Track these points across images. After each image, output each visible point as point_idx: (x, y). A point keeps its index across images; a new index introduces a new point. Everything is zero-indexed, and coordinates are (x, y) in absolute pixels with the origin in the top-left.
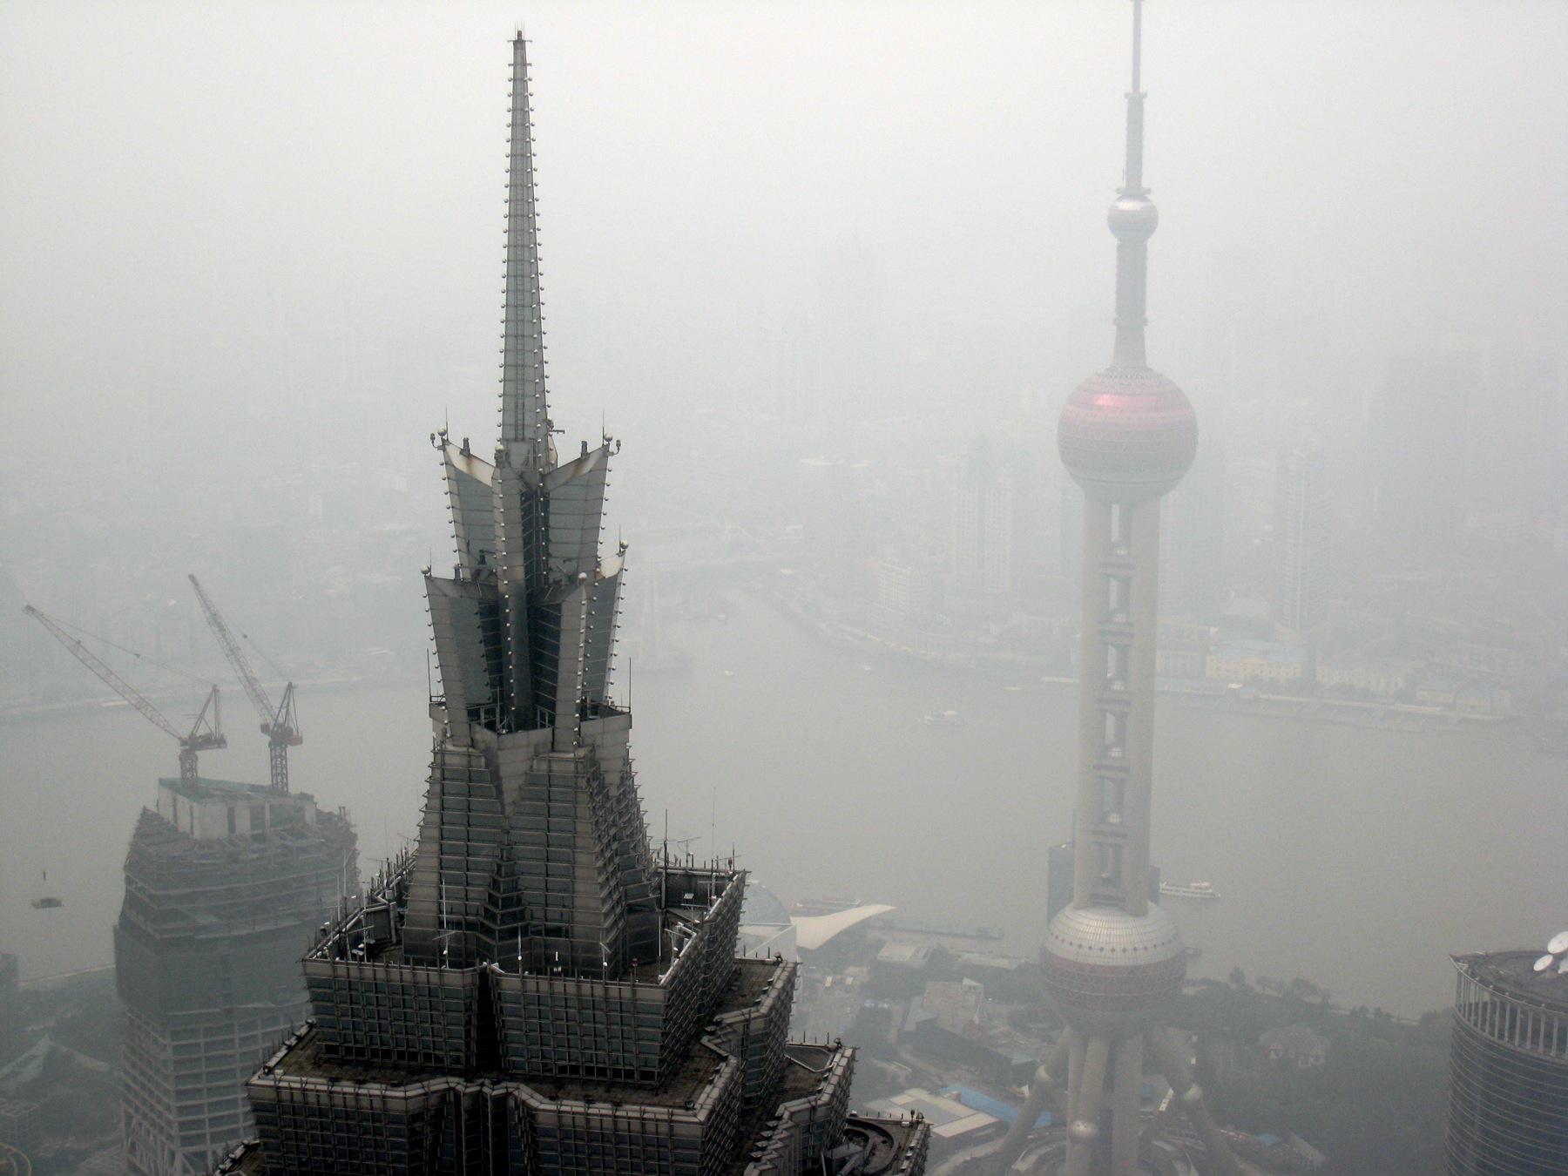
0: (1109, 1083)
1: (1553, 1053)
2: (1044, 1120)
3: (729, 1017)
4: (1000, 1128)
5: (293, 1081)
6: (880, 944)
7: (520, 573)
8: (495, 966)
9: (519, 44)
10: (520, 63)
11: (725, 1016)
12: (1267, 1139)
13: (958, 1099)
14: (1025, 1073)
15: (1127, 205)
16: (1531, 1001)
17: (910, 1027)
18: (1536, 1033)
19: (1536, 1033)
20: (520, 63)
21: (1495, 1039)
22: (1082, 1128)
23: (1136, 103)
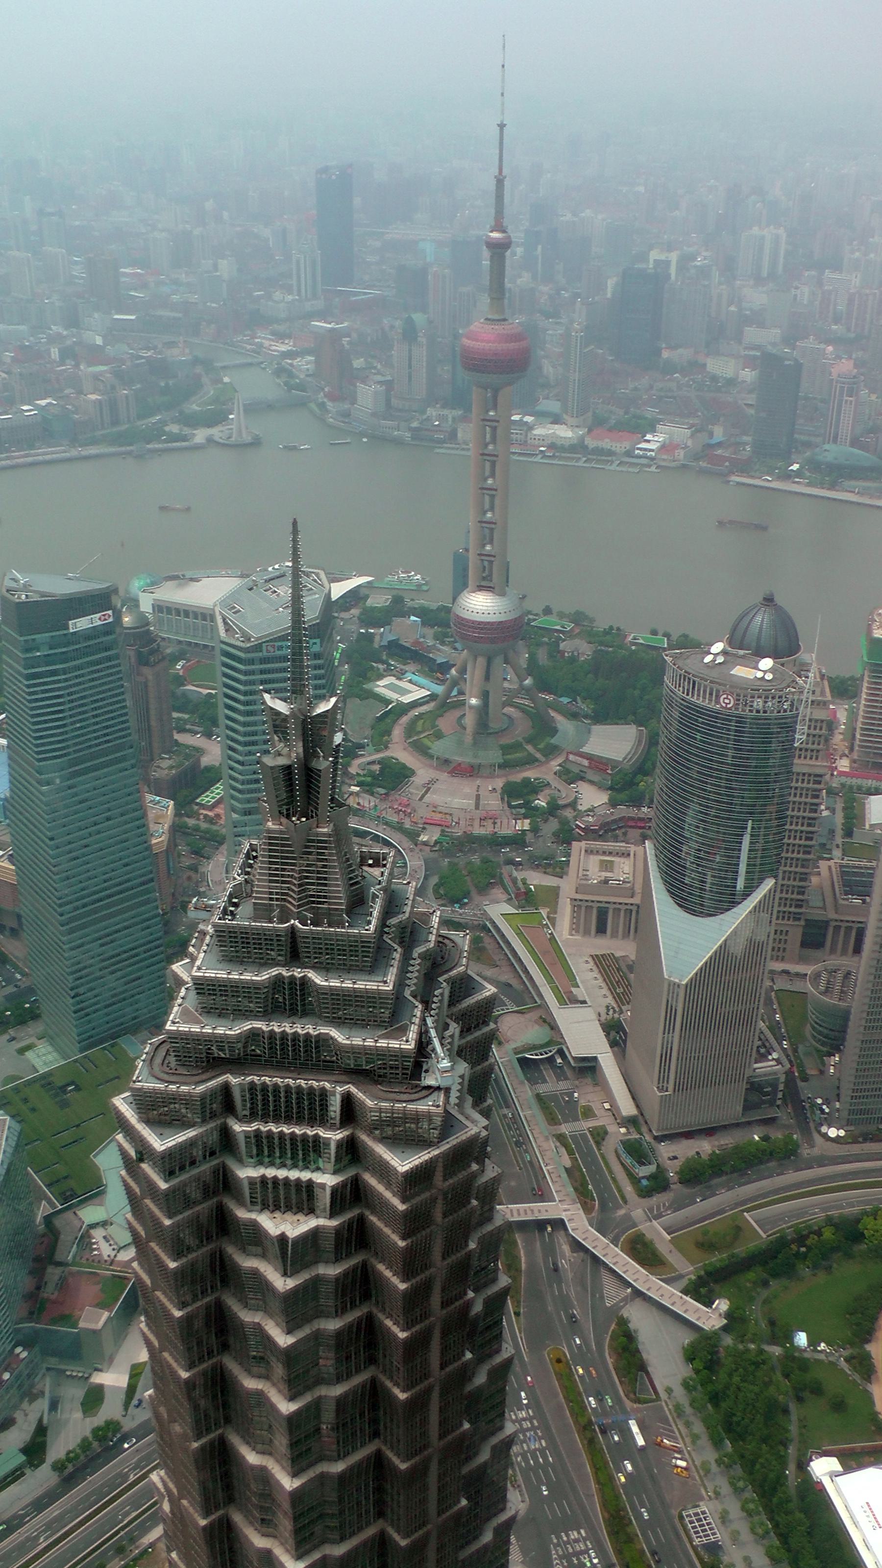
0: (487, 678)
1: (713, 703)
2: (454, 693)
3: (393, 921)
4: (433, 697)
5: (211, 974)
6: (366, 597)
7: (301, 750)
8: (297, 923)
9: (295, 523)
10: (295, 531)
11: (391, 920)
12: (565, 700)
13: (410, 681)
14: (444, 668)
15: (495, 235)
16: (702, 679)
17: (385, 643)
18: (705, 691)
19: (705, 691)
20: (295, 531)
21: (685, 695)
22: (474, 701)
23: (500, 182)
